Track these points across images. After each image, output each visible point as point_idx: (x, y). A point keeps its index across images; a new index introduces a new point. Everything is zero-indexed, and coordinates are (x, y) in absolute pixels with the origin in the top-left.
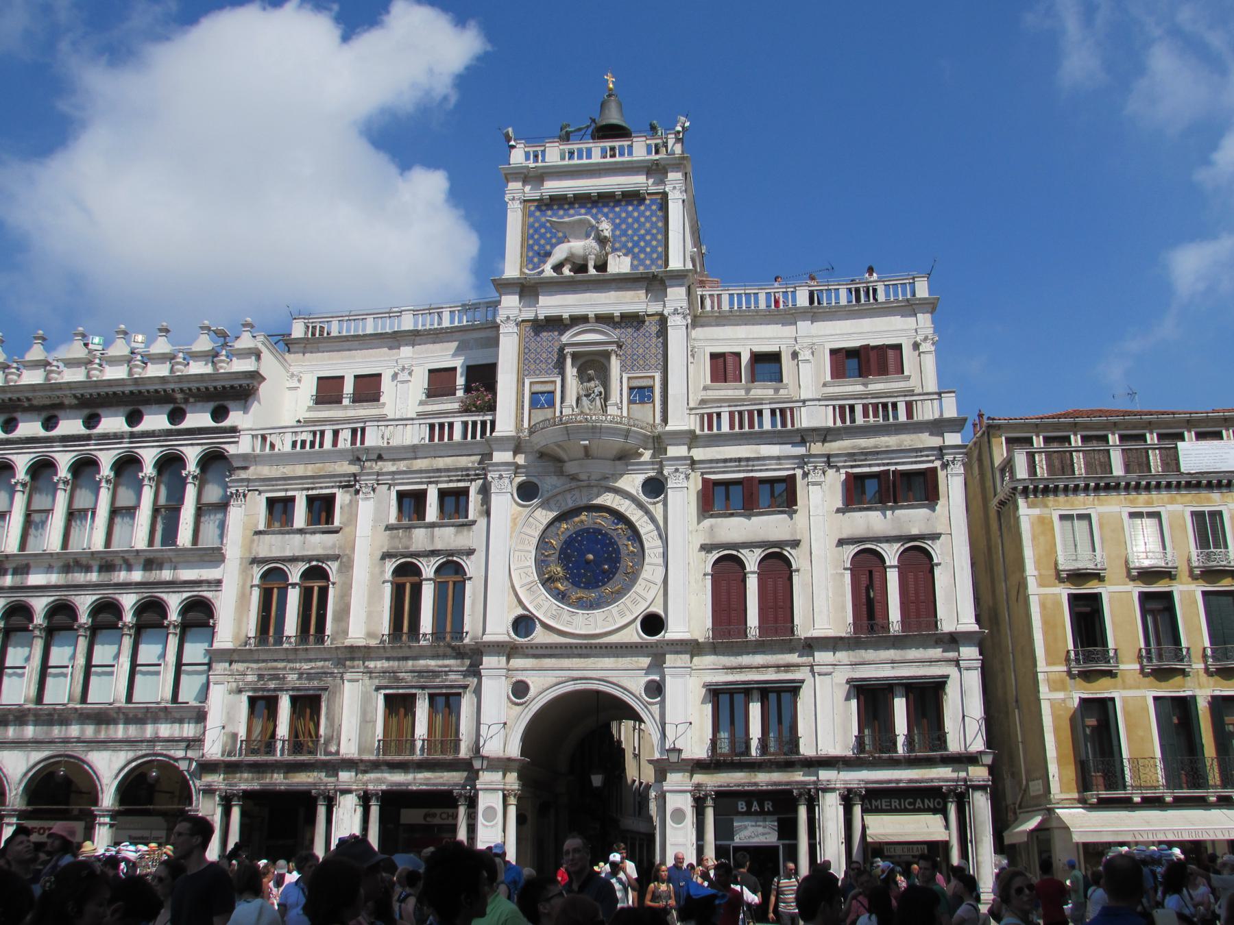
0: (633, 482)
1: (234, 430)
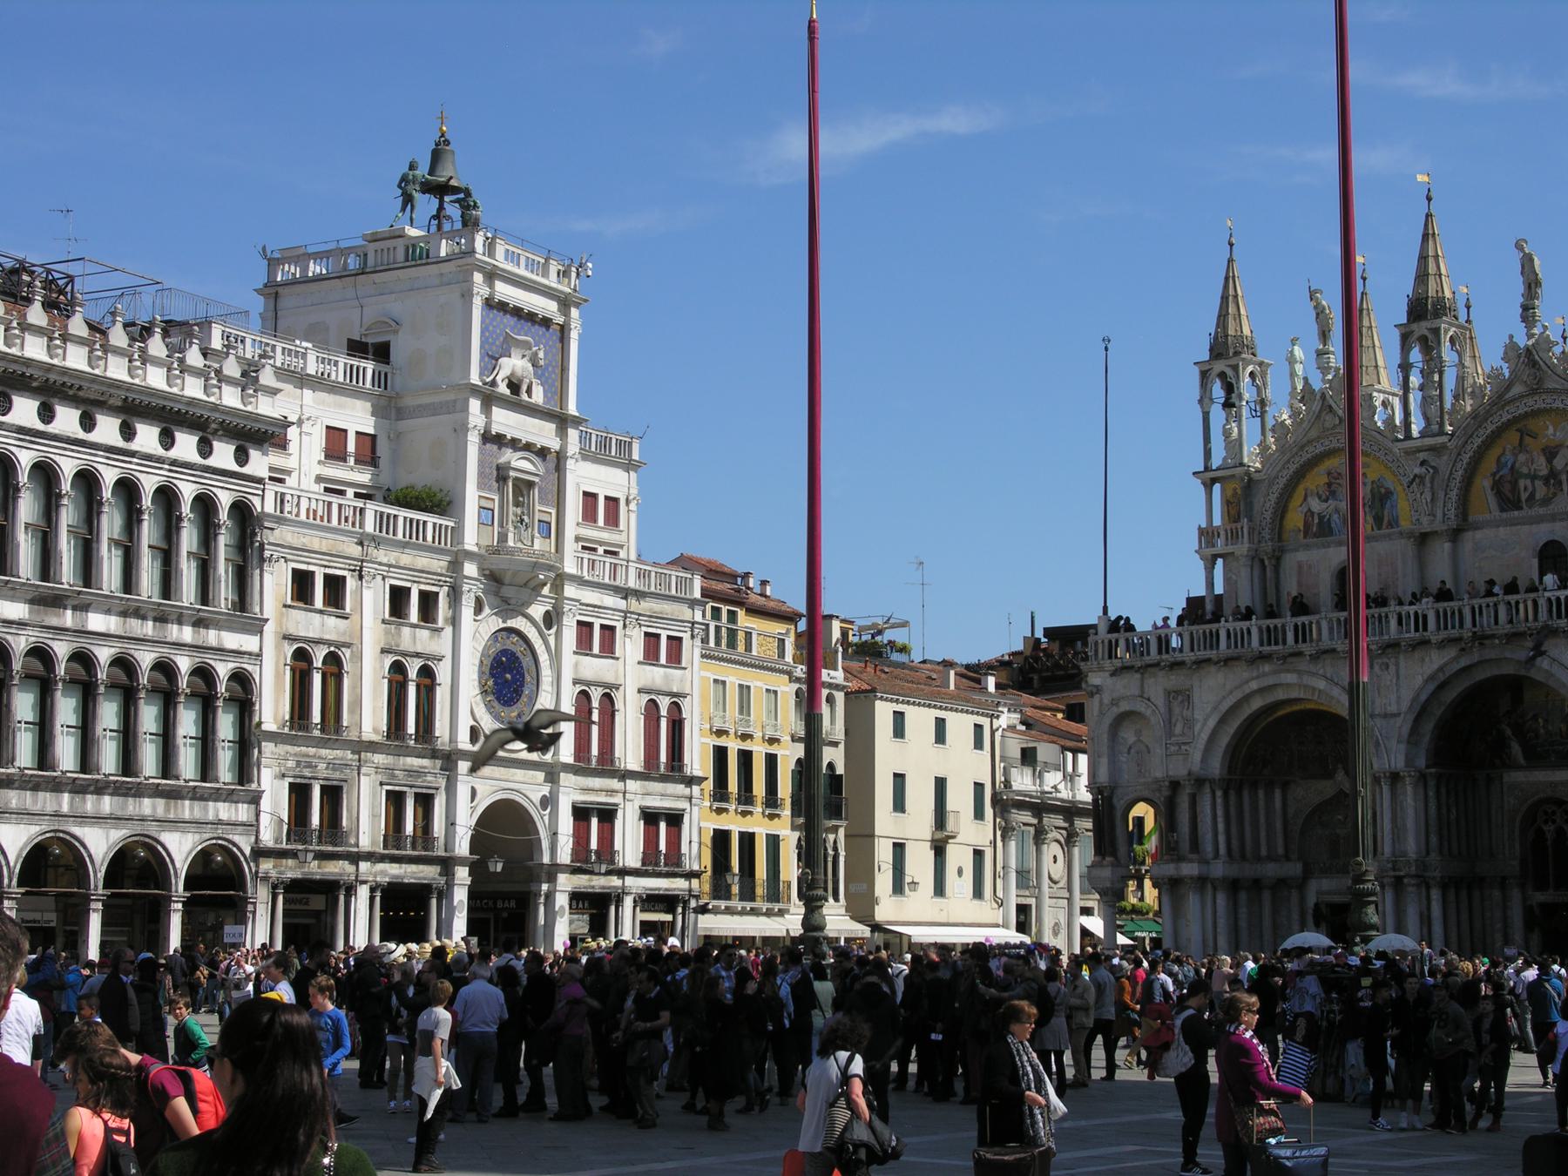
0: (537, 611)
1: (260, 481)
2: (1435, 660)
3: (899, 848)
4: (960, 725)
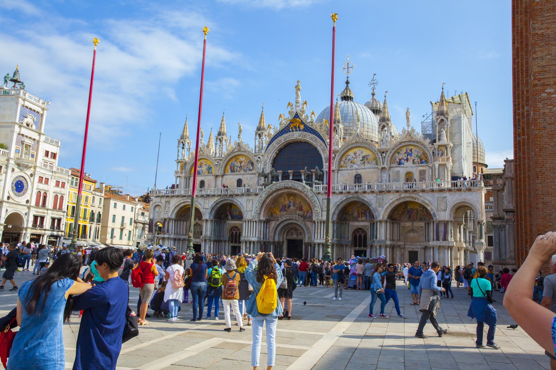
2: (216, 199)
3: (113, 230)
4: (129, 206)
